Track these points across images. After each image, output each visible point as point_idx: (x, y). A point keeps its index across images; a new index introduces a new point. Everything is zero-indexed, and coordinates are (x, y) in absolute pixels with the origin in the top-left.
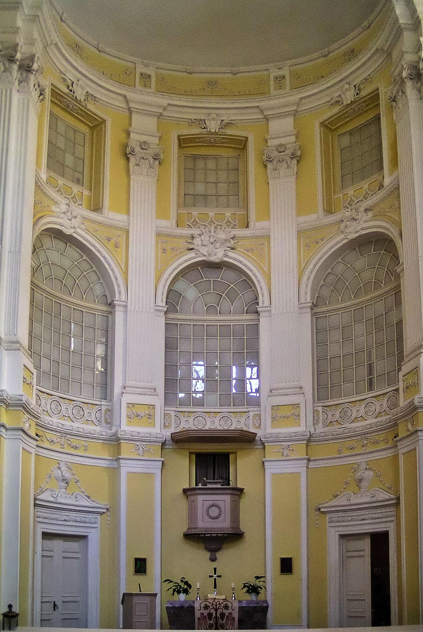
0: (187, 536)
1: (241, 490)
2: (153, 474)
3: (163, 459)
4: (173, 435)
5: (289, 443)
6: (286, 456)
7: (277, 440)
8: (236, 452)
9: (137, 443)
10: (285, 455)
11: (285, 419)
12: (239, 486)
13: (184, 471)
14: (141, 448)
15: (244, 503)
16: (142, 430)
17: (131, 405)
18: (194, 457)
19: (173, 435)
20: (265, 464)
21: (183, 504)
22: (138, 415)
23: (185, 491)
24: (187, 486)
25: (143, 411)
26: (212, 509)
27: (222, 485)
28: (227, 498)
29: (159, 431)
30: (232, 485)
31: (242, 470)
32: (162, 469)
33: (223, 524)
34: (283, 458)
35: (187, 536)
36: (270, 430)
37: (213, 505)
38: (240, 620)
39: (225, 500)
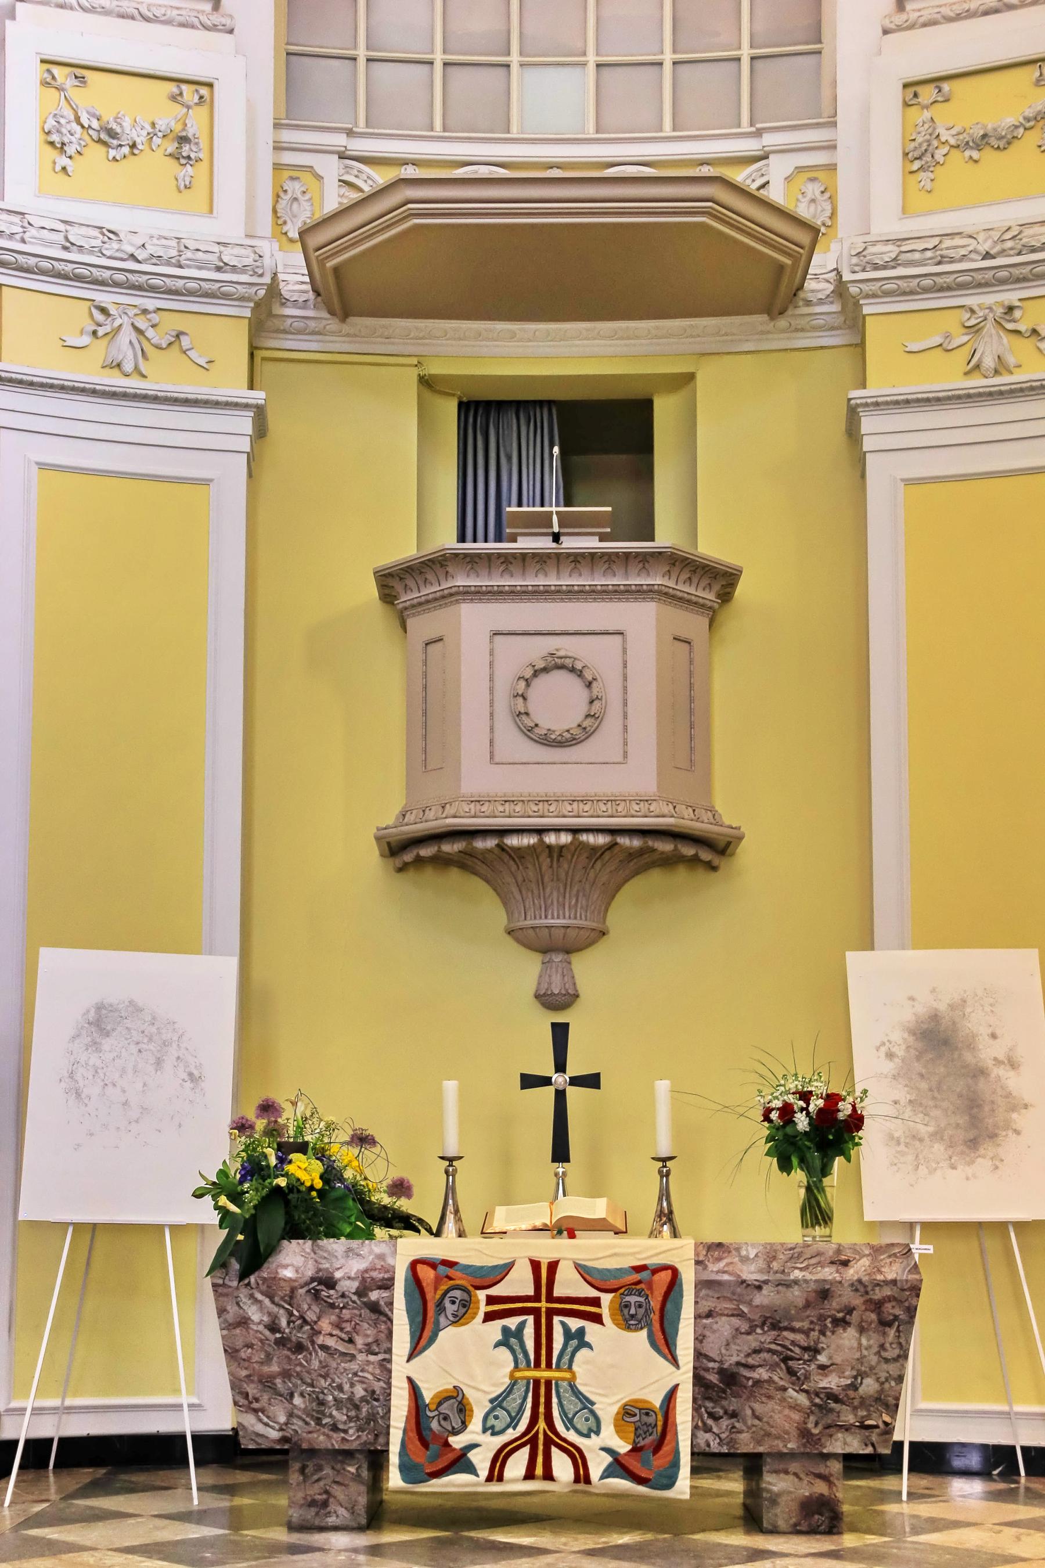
0: (411, 851)
1: (724, 580)
2: (206, 482)
3: (258, 396)
4: (317, 239)
5: (1012, 297)
6: (997, 372)
7: (935, 279)
8: (691, 377)
9: (104, 298)
10: (989, 362)
11: (988, 156)
12: (709, 547)
13: (390, 478)
14: (127, 335)
15: (735, 670)
16: (136, 214)
17: (63, 72)
18: (449, 411)
19: (317, 239)
20: (868, 424)
21: (383, 667)
22: (108, 136)
23: (391, 582)
24: (405, 549)
25: (142, 110)
26: (555, 695)
27: (603, 538)
28: (642, 620)
29: (235, 232)
30: (666, 535)
31: (727, 469)
32: (251, 458)
33: (620, 780)
34: (977, 382)
35: (411, 851)
36: (888, 222)
37: (556, 664)
38: (696, 1487)
39: (631, 634)
